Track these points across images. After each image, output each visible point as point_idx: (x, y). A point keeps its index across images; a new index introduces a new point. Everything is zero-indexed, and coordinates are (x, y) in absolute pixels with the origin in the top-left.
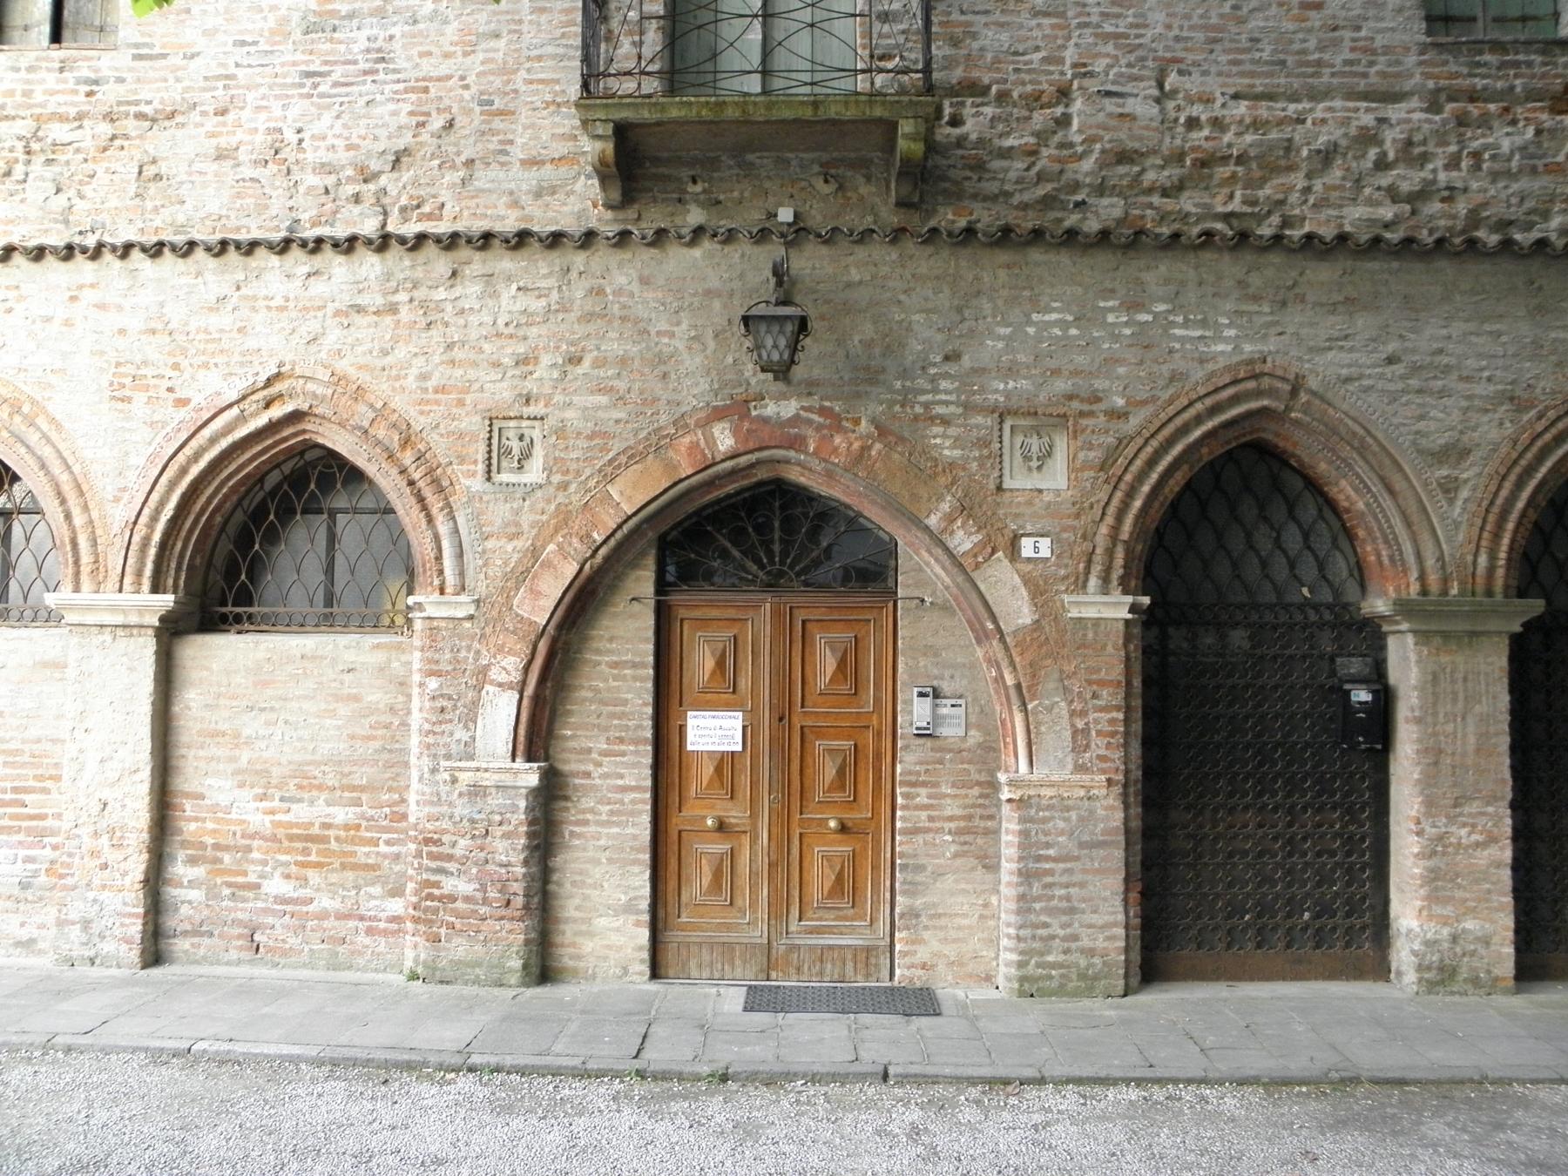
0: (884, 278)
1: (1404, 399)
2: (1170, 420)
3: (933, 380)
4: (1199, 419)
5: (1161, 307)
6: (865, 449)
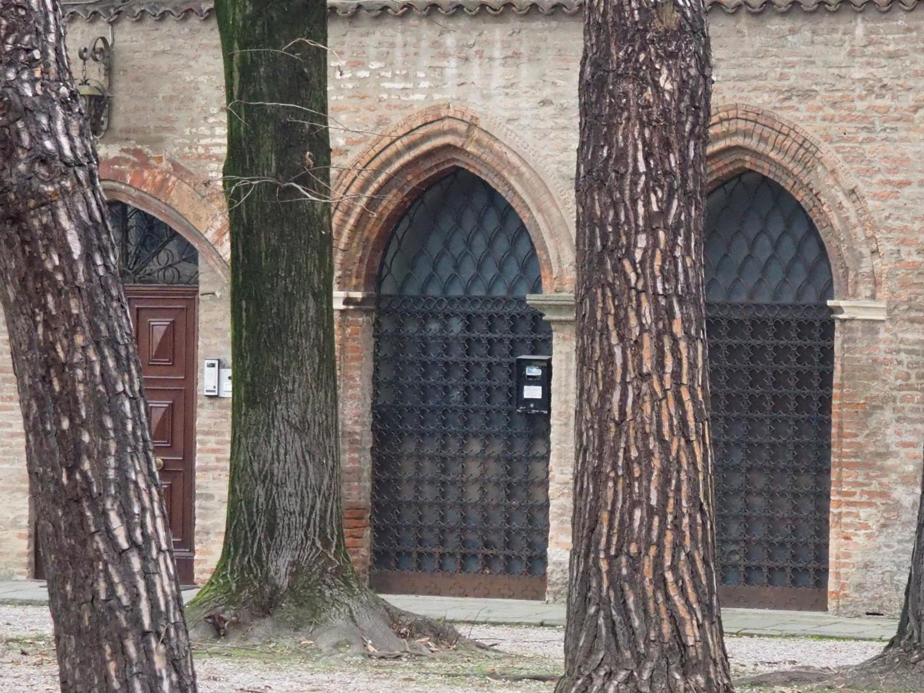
0: (181, 47)
1: (552, 136)
2: (377, 155)
3: (212, 128)
4: (398, 154)
5: (375, 65)
6: (165, 180)
